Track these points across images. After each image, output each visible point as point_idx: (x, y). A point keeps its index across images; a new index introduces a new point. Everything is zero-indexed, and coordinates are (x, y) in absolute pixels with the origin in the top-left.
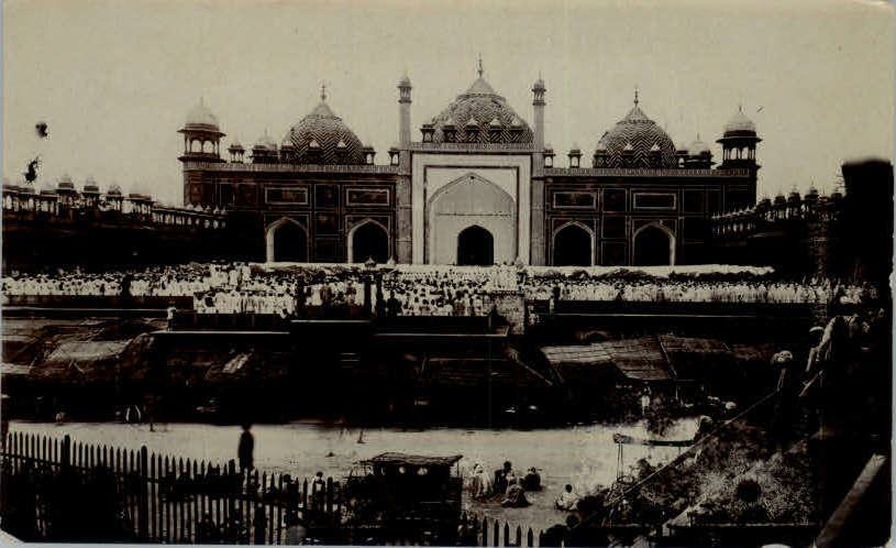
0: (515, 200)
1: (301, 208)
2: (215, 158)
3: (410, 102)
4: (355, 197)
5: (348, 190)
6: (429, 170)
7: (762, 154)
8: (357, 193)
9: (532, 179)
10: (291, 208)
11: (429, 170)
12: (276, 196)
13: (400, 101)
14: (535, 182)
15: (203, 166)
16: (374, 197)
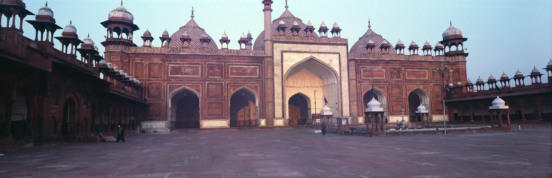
0: (339, 74)
1: (195, 79)
2: (130, 44)
3: (272, 10)
4: (234, 71)
5: (230, 66)
6: (284, 54)
7: (466, 46)
8: (236, 69)
9: (349, 61)
10: (189, 80)
11: (284, 54)
12: (176, 71)
13: (264, 11)
14: (350, 62)
15: (118, 49)
16: (249, 71)
